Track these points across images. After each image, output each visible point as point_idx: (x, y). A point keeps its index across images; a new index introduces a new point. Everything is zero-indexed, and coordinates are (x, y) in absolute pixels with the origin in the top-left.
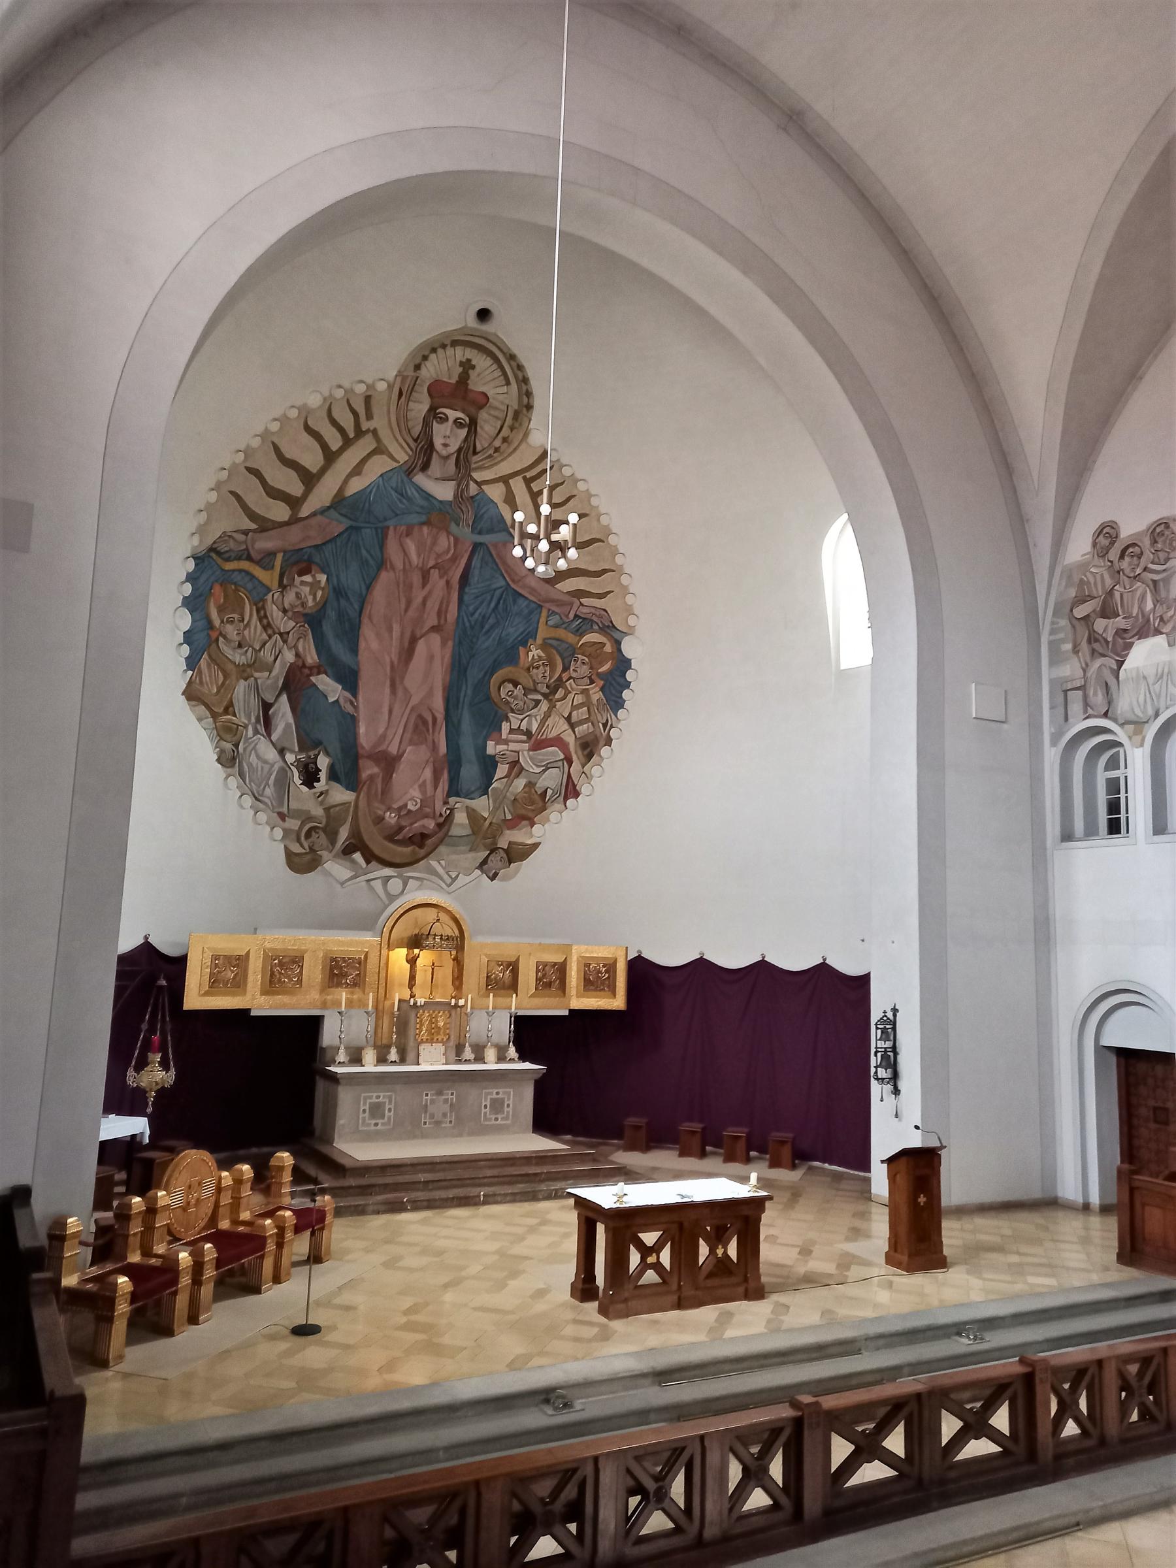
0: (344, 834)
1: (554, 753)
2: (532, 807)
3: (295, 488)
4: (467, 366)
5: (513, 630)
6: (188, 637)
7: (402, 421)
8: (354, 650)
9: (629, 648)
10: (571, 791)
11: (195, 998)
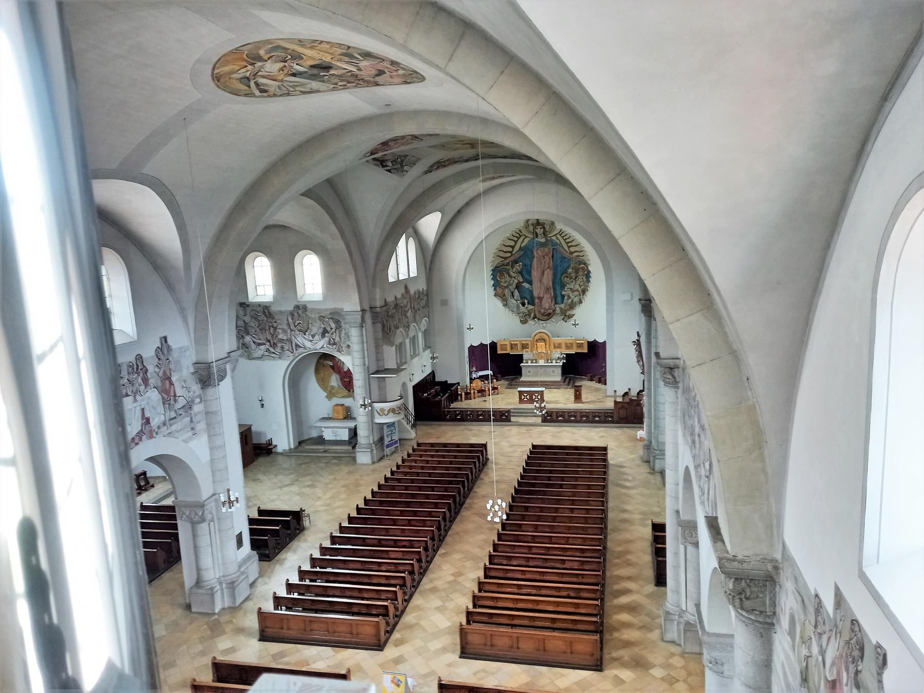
0: (532, 315)
1: (577, 293)
2: (572, 306)
3: (510, 249)
5: (565, 265)
6: (494, 285)
7: (529, 232)
9: (590, 268)
10: (581, 302)
11: (499, 352)
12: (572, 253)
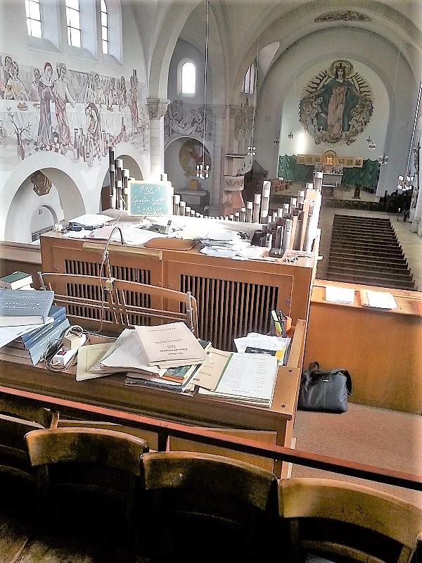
0: (324, 139)
2: (356, 133)
3: (316, 86)
4: (341, 64)
8: (327, 108)
12: (361, 93)
